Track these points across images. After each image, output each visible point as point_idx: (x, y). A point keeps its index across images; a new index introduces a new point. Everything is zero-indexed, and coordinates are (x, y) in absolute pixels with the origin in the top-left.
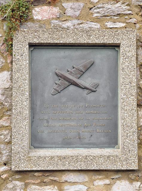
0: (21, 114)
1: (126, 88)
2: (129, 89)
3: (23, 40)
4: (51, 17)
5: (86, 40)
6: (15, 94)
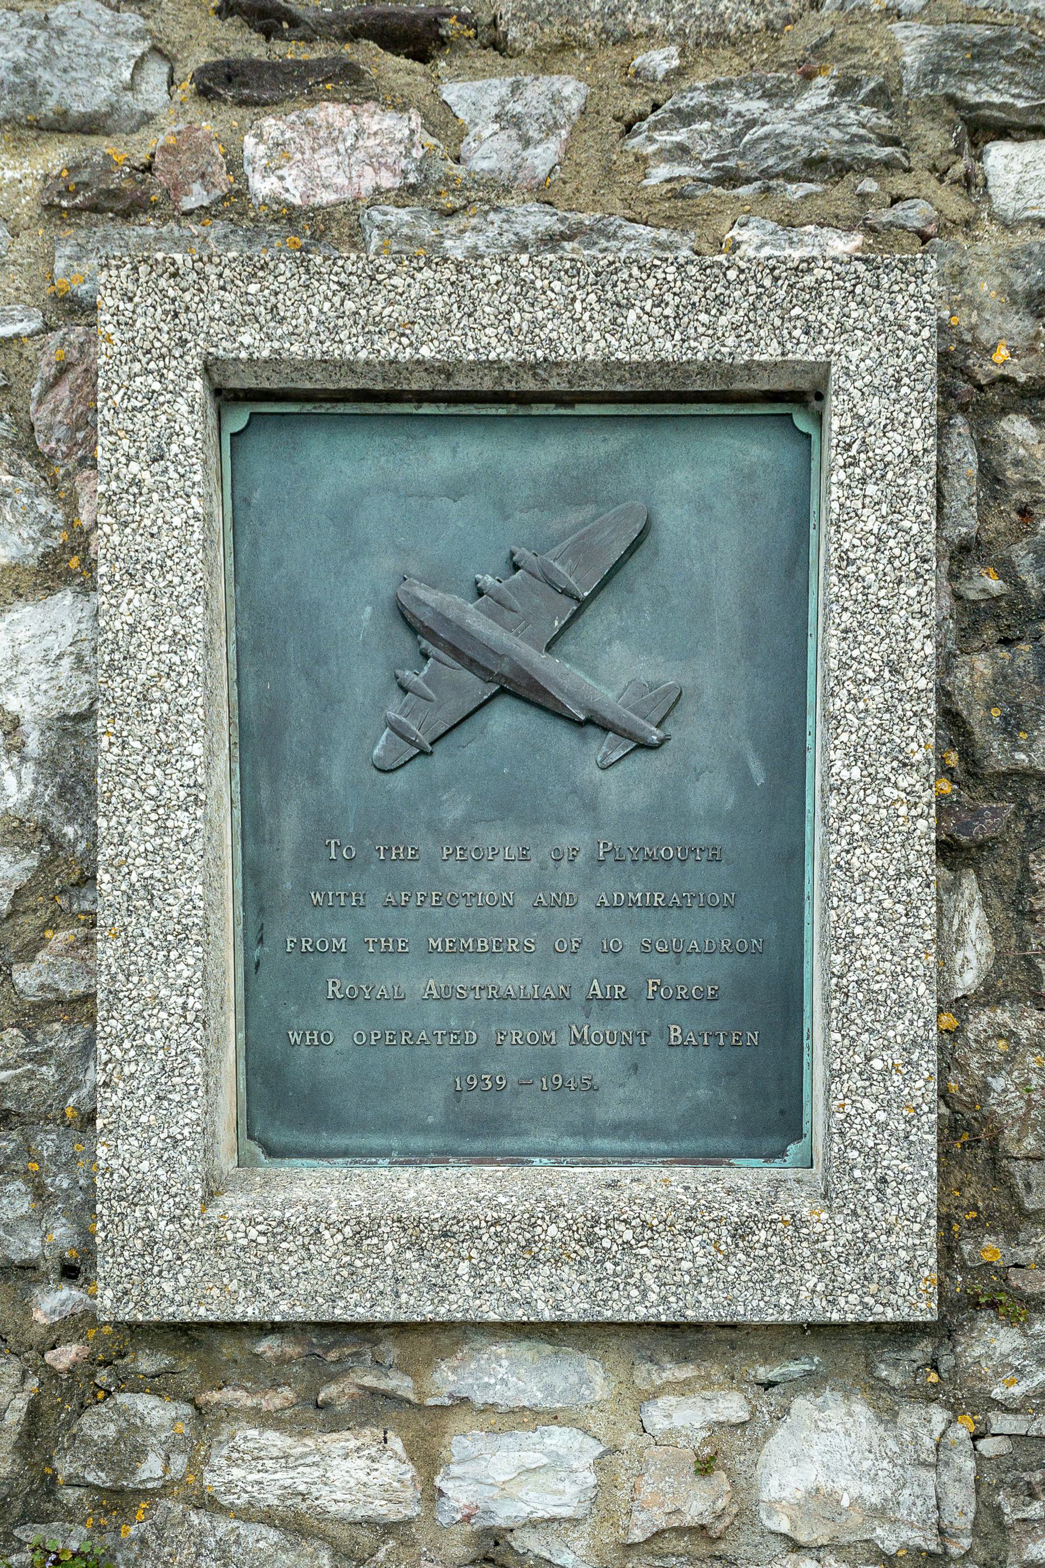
0: (157, 902)
1: (861, 705)
2: (887, 716)
3: (165, 338)
4: (368, 181)
5: (597, 336)
6: (114, 750)
